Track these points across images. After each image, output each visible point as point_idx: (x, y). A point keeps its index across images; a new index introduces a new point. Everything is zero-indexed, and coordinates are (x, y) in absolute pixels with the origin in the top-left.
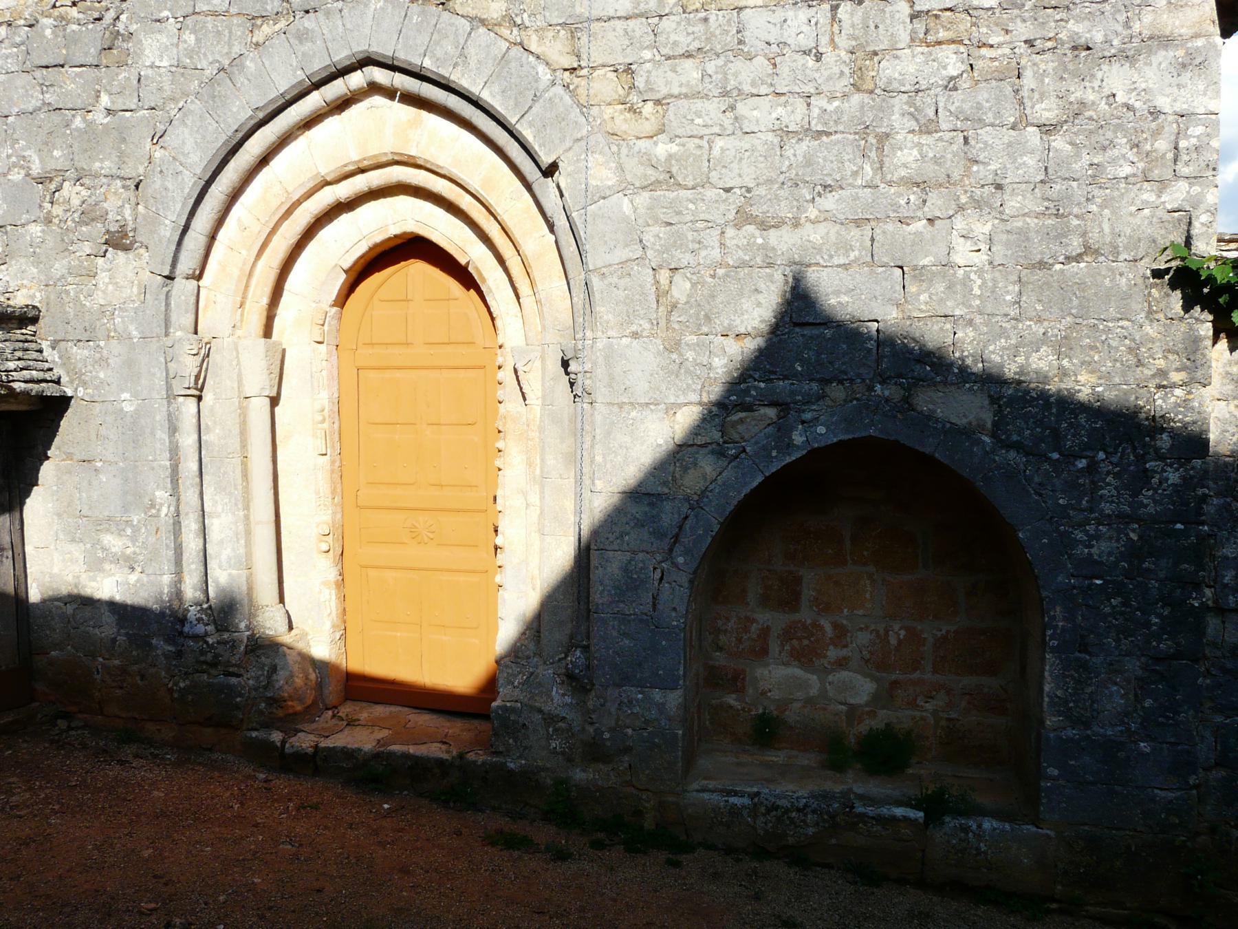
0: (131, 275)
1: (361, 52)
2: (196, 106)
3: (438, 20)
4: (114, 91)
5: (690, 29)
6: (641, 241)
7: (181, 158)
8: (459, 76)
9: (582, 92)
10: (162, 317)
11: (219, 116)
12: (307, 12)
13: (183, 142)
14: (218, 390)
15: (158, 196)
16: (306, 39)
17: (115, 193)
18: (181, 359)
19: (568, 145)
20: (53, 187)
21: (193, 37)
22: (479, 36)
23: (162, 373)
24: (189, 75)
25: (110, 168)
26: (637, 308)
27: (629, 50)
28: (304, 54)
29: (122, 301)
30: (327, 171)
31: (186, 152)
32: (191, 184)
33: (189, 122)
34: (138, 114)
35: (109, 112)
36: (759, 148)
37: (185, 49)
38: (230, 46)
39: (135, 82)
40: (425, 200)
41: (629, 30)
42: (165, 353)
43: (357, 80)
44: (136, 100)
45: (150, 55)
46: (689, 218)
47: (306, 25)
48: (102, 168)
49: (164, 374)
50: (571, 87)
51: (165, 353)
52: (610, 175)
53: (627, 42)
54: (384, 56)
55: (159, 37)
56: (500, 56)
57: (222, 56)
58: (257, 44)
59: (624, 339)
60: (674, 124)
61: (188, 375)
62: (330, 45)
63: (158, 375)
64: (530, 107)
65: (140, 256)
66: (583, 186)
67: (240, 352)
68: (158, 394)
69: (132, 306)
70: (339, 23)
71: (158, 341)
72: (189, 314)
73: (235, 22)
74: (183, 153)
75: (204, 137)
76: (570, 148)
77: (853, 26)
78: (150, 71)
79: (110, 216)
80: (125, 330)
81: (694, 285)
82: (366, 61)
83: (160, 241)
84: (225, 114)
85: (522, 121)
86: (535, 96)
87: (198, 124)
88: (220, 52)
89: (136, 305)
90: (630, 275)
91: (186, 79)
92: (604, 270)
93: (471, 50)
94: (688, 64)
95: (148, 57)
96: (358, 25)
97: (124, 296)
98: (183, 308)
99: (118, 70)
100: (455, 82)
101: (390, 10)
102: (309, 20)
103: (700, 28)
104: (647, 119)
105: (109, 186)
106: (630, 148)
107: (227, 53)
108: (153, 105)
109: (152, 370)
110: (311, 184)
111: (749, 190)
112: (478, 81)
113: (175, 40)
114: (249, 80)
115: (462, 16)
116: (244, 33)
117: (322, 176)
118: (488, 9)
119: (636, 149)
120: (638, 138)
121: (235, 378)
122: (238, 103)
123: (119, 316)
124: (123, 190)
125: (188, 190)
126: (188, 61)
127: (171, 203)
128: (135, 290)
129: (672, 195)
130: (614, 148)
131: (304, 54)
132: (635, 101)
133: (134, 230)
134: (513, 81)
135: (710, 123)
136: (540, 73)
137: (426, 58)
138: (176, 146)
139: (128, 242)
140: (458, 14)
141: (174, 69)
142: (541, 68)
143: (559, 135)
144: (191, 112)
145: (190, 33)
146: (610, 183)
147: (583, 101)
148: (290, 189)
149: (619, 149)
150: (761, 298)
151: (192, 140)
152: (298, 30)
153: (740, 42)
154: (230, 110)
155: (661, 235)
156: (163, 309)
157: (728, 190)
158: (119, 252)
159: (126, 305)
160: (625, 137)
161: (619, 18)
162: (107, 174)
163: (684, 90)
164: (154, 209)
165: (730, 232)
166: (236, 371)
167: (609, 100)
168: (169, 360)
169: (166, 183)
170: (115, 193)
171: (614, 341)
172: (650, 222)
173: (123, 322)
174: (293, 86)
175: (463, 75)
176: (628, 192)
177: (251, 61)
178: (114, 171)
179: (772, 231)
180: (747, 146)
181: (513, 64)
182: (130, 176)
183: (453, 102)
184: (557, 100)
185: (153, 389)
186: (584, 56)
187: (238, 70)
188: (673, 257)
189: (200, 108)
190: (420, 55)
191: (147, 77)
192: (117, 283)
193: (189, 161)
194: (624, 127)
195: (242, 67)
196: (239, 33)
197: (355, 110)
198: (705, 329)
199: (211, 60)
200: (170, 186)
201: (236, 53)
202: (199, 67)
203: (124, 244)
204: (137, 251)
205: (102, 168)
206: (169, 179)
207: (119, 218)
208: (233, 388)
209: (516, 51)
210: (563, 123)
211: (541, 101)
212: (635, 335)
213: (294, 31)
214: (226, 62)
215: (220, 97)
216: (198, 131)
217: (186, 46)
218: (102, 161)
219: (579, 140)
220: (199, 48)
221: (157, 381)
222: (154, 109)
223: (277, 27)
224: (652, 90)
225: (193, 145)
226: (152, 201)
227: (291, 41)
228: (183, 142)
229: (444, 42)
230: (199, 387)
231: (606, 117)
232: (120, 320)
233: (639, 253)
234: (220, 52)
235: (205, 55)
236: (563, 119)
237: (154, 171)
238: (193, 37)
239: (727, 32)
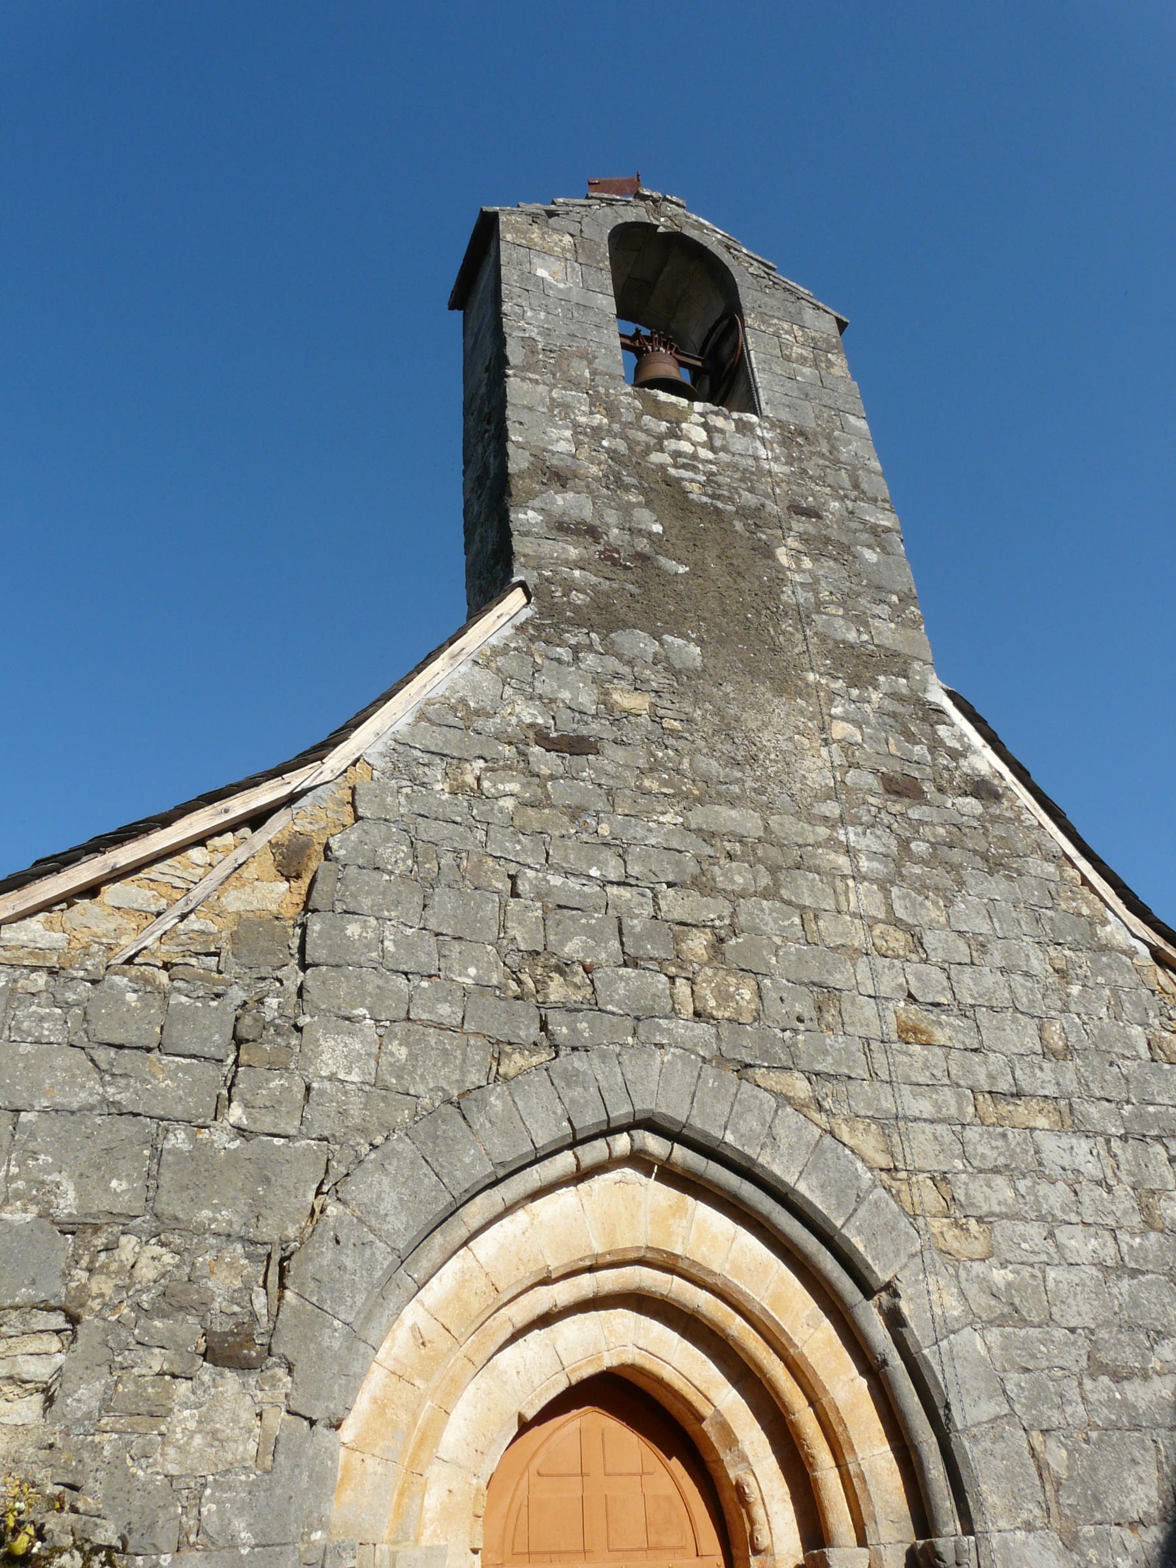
0: (247, 1416)
1: (644, 1111)
2: (404, 1147)
3: (738, 1090)
4: (259, 1102)
5: (994, 1143)
6: (1004, 1391)
7: (373, 1222)
8: (769, 1159)
9: (905, 1197)
11: (442, 1166)
12: (574, 1049)
13: (379, 1196)
15: (325, 1278)
16: (575, 1082)
17: (230, 1265)
19: (904, 1260)
20: (100, 1241)
21: (404, 1051)
22: (787, 1116)
24: (395, 1100)
25: (230, 1223)
26: (1022, 1485)
27: (941, 1157)
28: (572, 1101)
29: (221, 1467)
30: (557, 1265)
31: (383, 1212)
32: (386, 1264)
33: (391, 1169)
34: (297, 1144)
35: (240, 1131)
36: (1088, 1283)
37: (391, 1065)
38: (464, 1073)
39: (300, 1096)
40: (653, 1317)
41: (938, 1134)
43: (622, 1144)
44: (297, 1123)
45: (330, 1062)
46: (1045, 1364)
47: (576, 1065)
48: (214, 1220)
50: (894, 1191)
52: (954, 1303)
53: (938, 1147)
54: (673, 1120)
55: (347, 1040)
56: (813, 1143)
57: (449, 1083)
58: (506, 1079)
59: (1018, 1532)
60: (1004, 1246)
62: (606, 1095)
64: (855, 1210)
65: (274, 1382)
66: (929, 1315)
69: (243, 1478)
70: (618, 1070)
73: (472, 1042)
74: (377, 1215)
75: (415, 1194)
76: (906, 1266)
77: (1128, 1162)
78: (327, 1085)
79: (216, 1305)
80: (225, 1525)
81: (1070, 1452)
82: (651, 1124)
83: (320, 1356)
84: (451, 1164)
85: (848, 1225)
86: (858, 1196)
87: (407, 1172)
88: (446, 1078)
89: (252, 1476)
90: (1002, 1437)
91: (388, 1105)
92: (975, 1430)
93: (780, 1131)
94: (1000, 1181)
95: (327, 1065)
96: (642, 1079)
97: (230, 1457)
99: (269, 1074)
100: (763, 1166)
101: (679, 1066)
102: (580, 1059)
103: (1000, 1143)
104: (976, 1238)
105: (219, 1251)
106: (968, 1271)
107: (457, 1081)
108: (326, 1133)
110: (529, 1283)
111: (1092, 1332)
112: (792, 1169)
113: (375, 1050)
114: (490, 1122)
115: (766, 1090)
116: (484, 1059)
117: (550, 1272)
118: (794, 1086)
119: (974, 1273)
120: (972, 1260)
122: (472, 1152)
123: (212, 1499)
124: (247, 1261)
125: (380, 1273)
126: (394, 1081)
127: (348, 1292)
128: (252, 1447)
129: (1023, 1333)
130: (951, 1270)
131: (572, 1101)
132: (958, 1215)
133: (271, 1334)
134: (831, 1174)
135: (1036, 1249)
136: (859, 1169)
137: (728, 1132)
138: (365, 1200)
139: (254, 1354)
140: (759, 1086)
141: (367, 1088)
142: (859, 1165)
143: (892, 1247)
144: (396, 1154)
145: (400, 1045)
146: (956, 1313)
147: (909, 1209)
148: (501, 1286)
149: (957, 1272)
150: (1140, 1470)
151: (394, 1196)
152: (566, 1069)
153: (1040, 1164)
154: (460, 1161)
155: (1023, 1384)
157: (1073, 1330)
158: (228, 1373)
159: (231, 1477)
160: (958, 1257)
161: (925, 1120)
162: (221, 1231)
163: (1004, 1209)
164: (314, 1300)
165: (1088, 1384)
167: (934, 1211)
169: (343, 1258)
170: (230, 1265)
171: (1008, 1535)
172: (1007, 1367)
173: (221, 1512)
174: (555, 1141)
175: (774, 1160)
176: (978, 1326)
177: (497, 1098)
178: (236, 1227)
179: (1125, 1383)
180: (1077, 1280)
181: (829, 1155)
182: (266, 1239)
183: (747, 1190)
184: (883, 1205)
186: (900, 1157)
187: (477, 1106)
188: (1042, 1413)
189: (412, 1150)
190: (720, 1127)
191: (322, 1092)
192: (214, 1433)
193: (385, 1227)
194: (956, 1245)
195: (483, 1104)
196: (477, 1058)
197: (599, 1182)
198: (1098, 1516)
199: (431, 1085)
200: (349, 1264)
201: (473, 1083)
202: (412, 1092)
203: (245, 1357)
204: (269, 1373)
205: (214, 1220)
206: (349, 1252)
207: (236, 1309)
209: (828, 1139)
210: (894, 1234)
211: (866, 1203)
212: (1029, 1527)
213: (560, 1070)
214: (455, 1093)
215: (445, 1138)
216: (404, 1184)
217: (392, 1060)
218: (216, 1208)
219: (913, 1256)
220: (413, 1066)
222: (326, 1139)
223: (535, 1060)
224: (973, 1204)
225: (396, 1203)
226: (312, 1285)
227: (556, 1081)
228: (379, 1196)
229: (748, 1116)
231: (935, 1231)
232: (214, 1507)
233: (1005, 1410)
234: (446, 1078)
235: (422, 1077)
236: (893, 1229)
237: (322, 1237)
238: (404, 1051)
239: (1026, 1152)
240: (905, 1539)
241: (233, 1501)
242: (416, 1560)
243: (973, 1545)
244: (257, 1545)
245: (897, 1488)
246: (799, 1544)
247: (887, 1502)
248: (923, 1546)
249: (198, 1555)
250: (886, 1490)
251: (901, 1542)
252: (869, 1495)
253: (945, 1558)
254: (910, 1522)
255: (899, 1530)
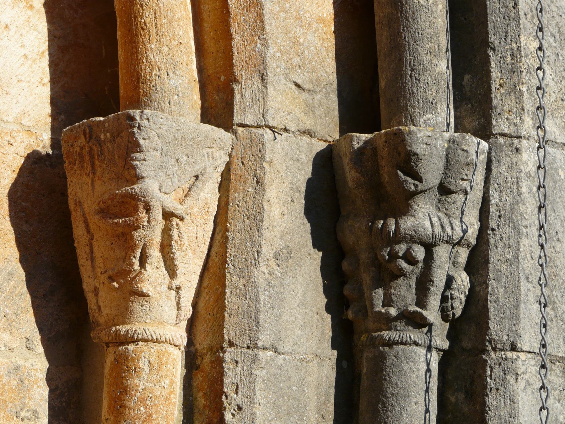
240: (320, 130)
243: (483, 157)
245: (320, 20)
246: (48, 109)
247: (295, 42)
248: (366, 142)
250: (298, 18)
251: (308, 133)
252: (260, 17)
253: (422, 169)
254: (334, 98)
255: (309, 109)
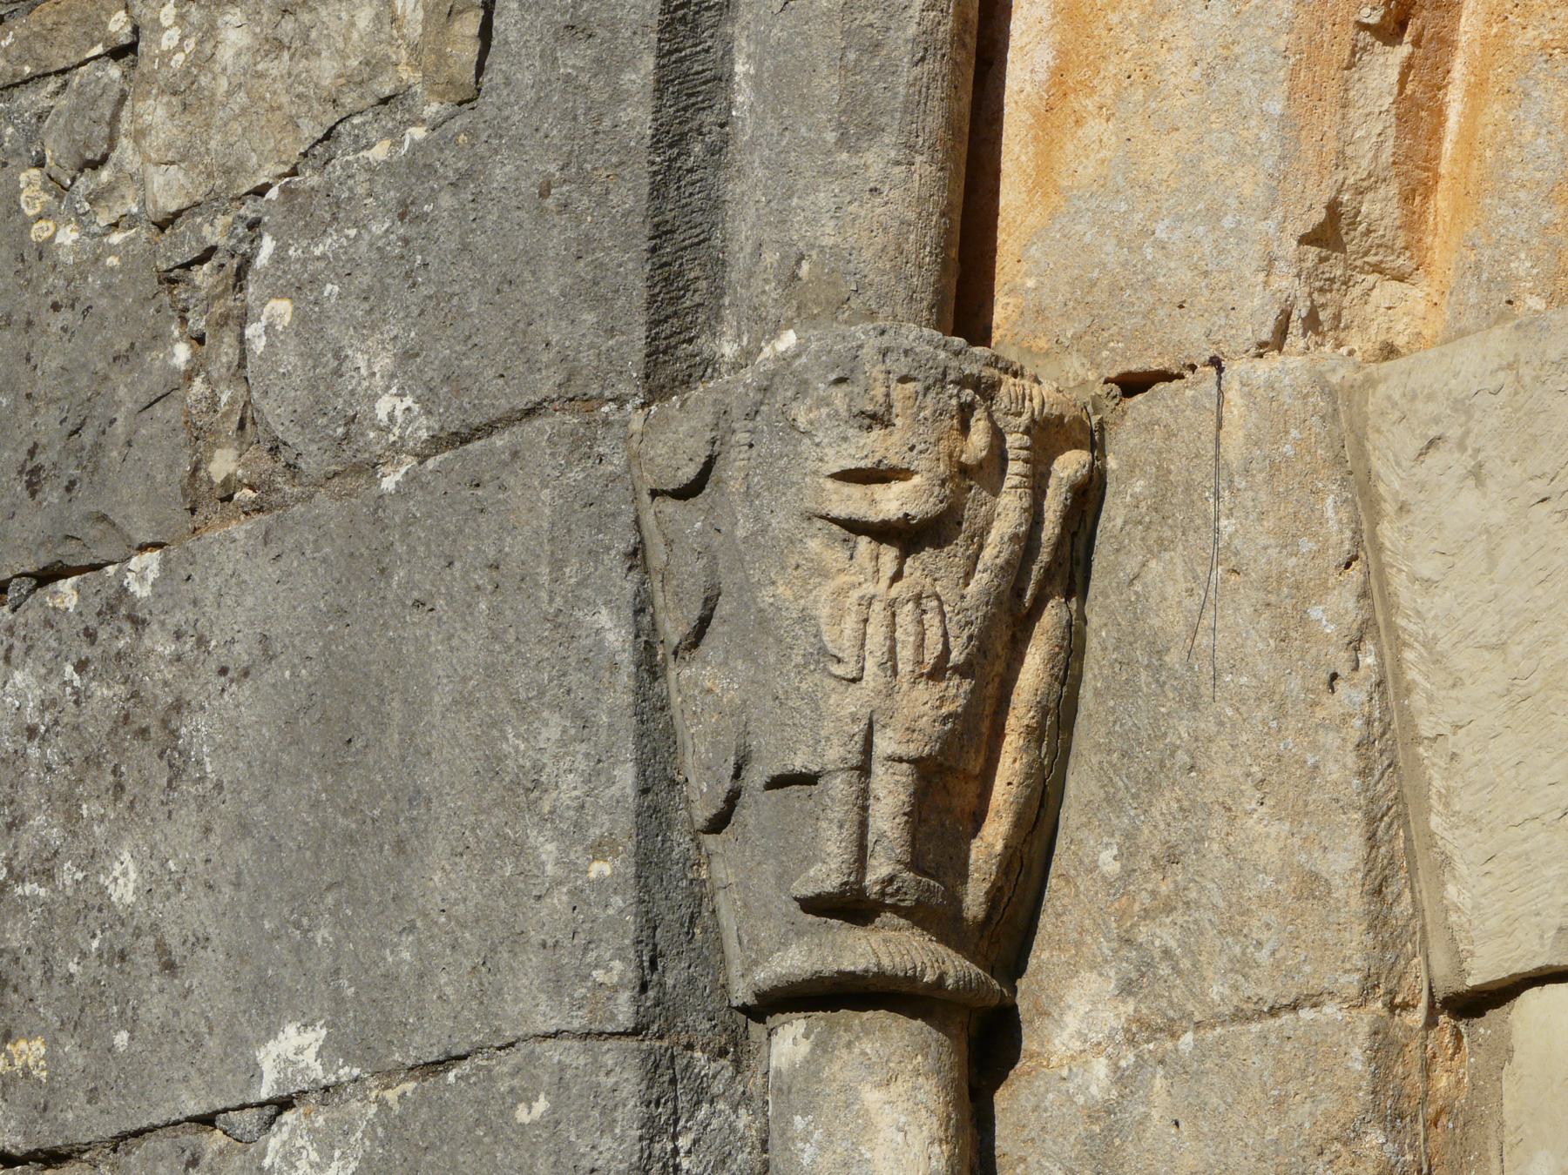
10: (630, 196)
14: (1162, 934)
18: (780, 592)
23: (597, 774)
42: (637, 555)
49: (626, 776)
51: (637, 555)
61: (836, 752)
63: (568, 790)
67: (1391, 482)
68: (556, 984)
71: (581, 446)
72: (876, 159)
98: (827, 84)
109: (512, 743)
121: (1340, 768)
156: (638, 118)
166: (1351, 695)
168: (674, 629)
173: (308, 324)
185: (517, 939)
208: (1312, 886)
221: (548, 850)
230: (974, 899)
241: (343, 266)
242: (1462, 406)
244: (437, 443)
249: (240, 529)
